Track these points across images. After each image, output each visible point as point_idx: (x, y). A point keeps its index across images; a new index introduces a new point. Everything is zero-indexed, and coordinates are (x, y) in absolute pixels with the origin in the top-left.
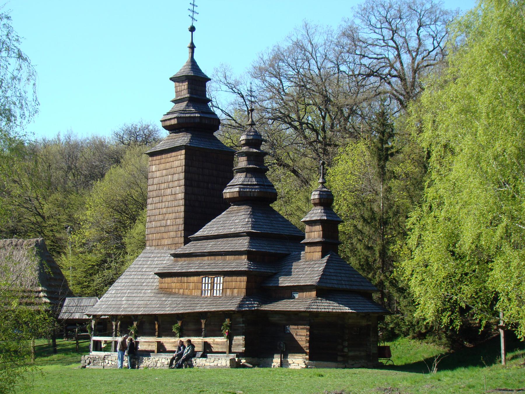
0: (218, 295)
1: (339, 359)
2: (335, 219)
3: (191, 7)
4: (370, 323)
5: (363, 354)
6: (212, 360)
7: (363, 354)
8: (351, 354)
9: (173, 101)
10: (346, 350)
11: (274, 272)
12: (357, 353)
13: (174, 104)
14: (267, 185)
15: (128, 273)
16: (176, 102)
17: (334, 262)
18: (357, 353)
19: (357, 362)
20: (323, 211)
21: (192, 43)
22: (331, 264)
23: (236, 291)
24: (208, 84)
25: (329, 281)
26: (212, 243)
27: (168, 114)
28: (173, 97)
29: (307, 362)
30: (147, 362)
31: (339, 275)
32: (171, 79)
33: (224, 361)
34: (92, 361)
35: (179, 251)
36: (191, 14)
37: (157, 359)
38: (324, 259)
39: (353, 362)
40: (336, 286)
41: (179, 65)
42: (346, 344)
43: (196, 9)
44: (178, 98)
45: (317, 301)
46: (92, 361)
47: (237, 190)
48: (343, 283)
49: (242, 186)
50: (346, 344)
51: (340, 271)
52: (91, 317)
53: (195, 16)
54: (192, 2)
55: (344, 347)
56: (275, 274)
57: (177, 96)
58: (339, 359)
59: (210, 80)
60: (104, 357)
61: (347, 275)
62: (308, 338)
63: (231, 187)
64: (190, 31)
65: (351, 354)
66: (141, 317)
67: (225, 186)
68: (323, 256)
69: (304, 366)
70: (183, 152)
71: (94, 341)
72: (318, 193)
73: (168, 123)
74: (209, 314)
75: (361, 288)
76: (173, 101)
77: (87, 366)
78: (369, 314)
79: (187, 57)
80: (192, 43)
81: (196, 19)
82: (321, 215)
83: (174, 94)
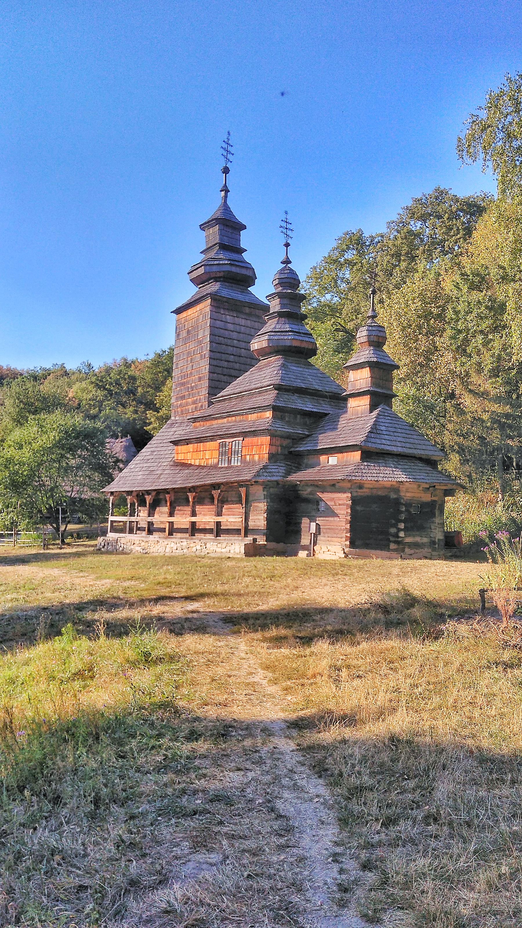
0: (236, 464)
1: (392, 546)
2: (389, 363)
4: (434, 498)
5: (425, 540)
6: (224, 545)
7: (425, 540)
8: (408, 540)
10: (402, 534)
11: (307, 433)
12: (418, 539)
14: (303, 333)
15: (151, 446)
18: (418, 539)
19: (417, 551)
20: (372, 352)
22: (383, 420)
25: (378, 441)
28: (205, 248)
29: (347, 550)
30: (156, 546)
31: (392, 434)
33: (236, 547)
34: (106, 544)
38: (372, 414)
39: (412, 552)
40: (388, 448)
41: (211, 209)
42: (402, 526)
43: (230, 148)
45: (362, 467)
46: (106, 544)
47: (266, 337)
48: (399, 444)
49: (272, 334)
50: (402, 526)
51: (394, 430)
53: (229, 156)
54: (226, 140)
55: (399, 530)
56: (308, 436)
57: (207, 245)
58: (392, 546)
59: (245, 227)
60: (117, 540)
62: (349, 518)
67: (252, 336)
68: (371, 412)
69: (343, 556)
70: (209, 301)
71: (112, 522)
72: (366, 328)
73: (195, 274)
75: (422, 452)
77: (102, 549)
78: (434, 486)
79: (219, 202)
82: (369, 356)
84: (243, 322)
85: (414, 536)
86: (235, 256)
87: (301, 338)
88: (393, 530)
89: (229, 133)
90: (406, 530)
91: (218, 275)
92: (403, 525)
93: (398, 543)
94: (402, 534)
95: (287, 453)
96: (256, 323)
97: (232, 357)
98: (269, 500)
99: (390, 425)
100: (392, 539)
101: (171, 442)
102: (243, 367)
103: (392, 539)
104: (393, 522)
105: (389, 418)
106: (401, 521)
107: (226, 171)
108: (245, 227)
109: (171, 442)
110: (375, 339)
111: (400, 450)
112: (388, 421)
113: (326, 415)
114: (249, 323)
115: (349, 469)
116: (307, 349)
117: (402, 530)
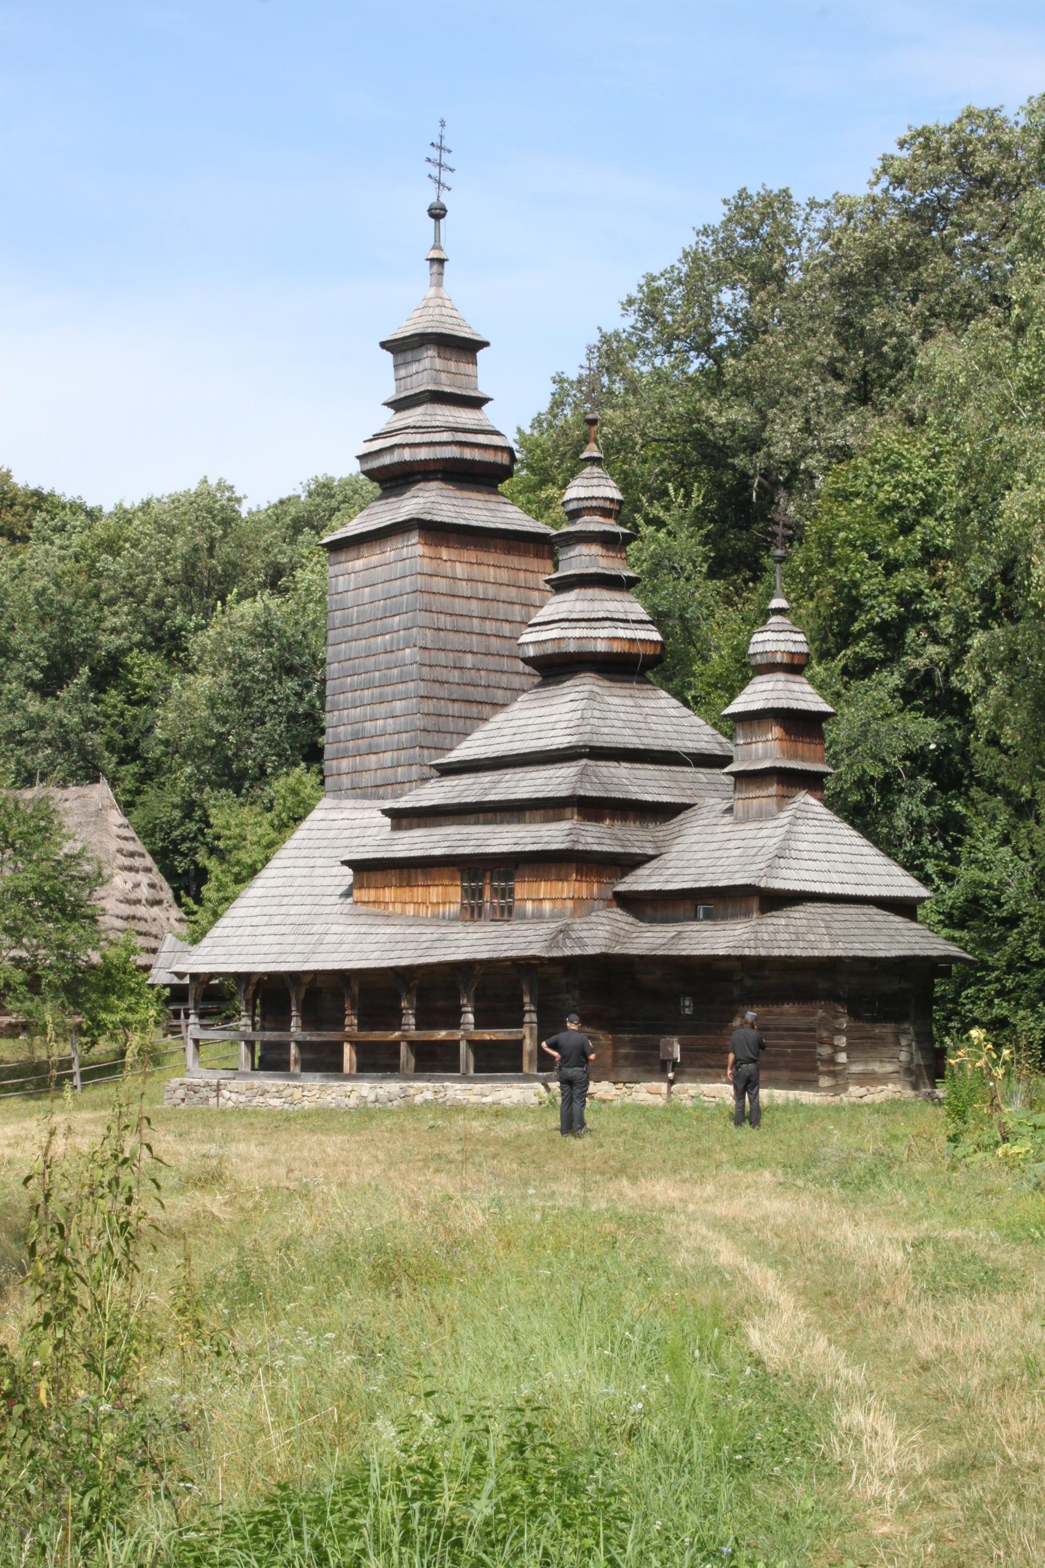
1: (825, 1082)
3: (434, 154)
5: (889, 1068)
8: (855, 1068)
9: (389, 404)
10: (842, 1058)
11: (651, 852)
13: (392, 411)
14: (634, 622)
16: (399, 405)
17: (811, 822)
18: (876, 1067)
19: (872, 1089)
21: (437, 247)
23: (547, 906)
24: (481, 355)
26: (486, 778)
27: (377, 437)
28: (391, 393)
32: (384, 345)
35: (404, 802)
36: (435, 171)
37: (349, 1088)
42: (842, 1041)
43: (446, 159)
44: (402, 395)
48: (835, 877)
50: (842, 1041)
52: (187, 981)
53: (446, 177)
54: (437, 141)
55: (837, 1049)
57: (398, 391)
59: (486, 344)
60: (219, 1085)
61: (848, 858)
63: (538, 628)
64: (432, 215)
65: (855, 1068)
66: (307, 979)
73: (375, 464)
74: (478, 967)
75: (885, 892)
76: (389, 404)
80: (437, 247)
81: (448, 184)
83: (393, 385)
84: (491, 573)
85: (866, 1062)
86: (464, 417)
87: (629, 634)
88: (825, 1051)
89: (443, 124)
90: (849, 1049)
91: (432, 467)
92: (844, 1039)
93: (833, 1074)
94: (842, 1058)
95: (610, 895)
96: (522, 575)
97: (469, 657)
98: (577, 994)
99: (816, 838)
100: (822, 1068)
101: (345, 863)
102: (500, 695)
103: (822, 1068)
104: (825, 1034)
105: (816, 822)
106: (839, 1032)
107: (437, 213)
108: (486, 344)
109: (345, 863)
110: (786, 660)
111: (839, 890)
112: (813, 830)
113: (687, 807)
114: (504, 575)
115: (737, 933)
116: (645, 655)
117: (843, 1050)
